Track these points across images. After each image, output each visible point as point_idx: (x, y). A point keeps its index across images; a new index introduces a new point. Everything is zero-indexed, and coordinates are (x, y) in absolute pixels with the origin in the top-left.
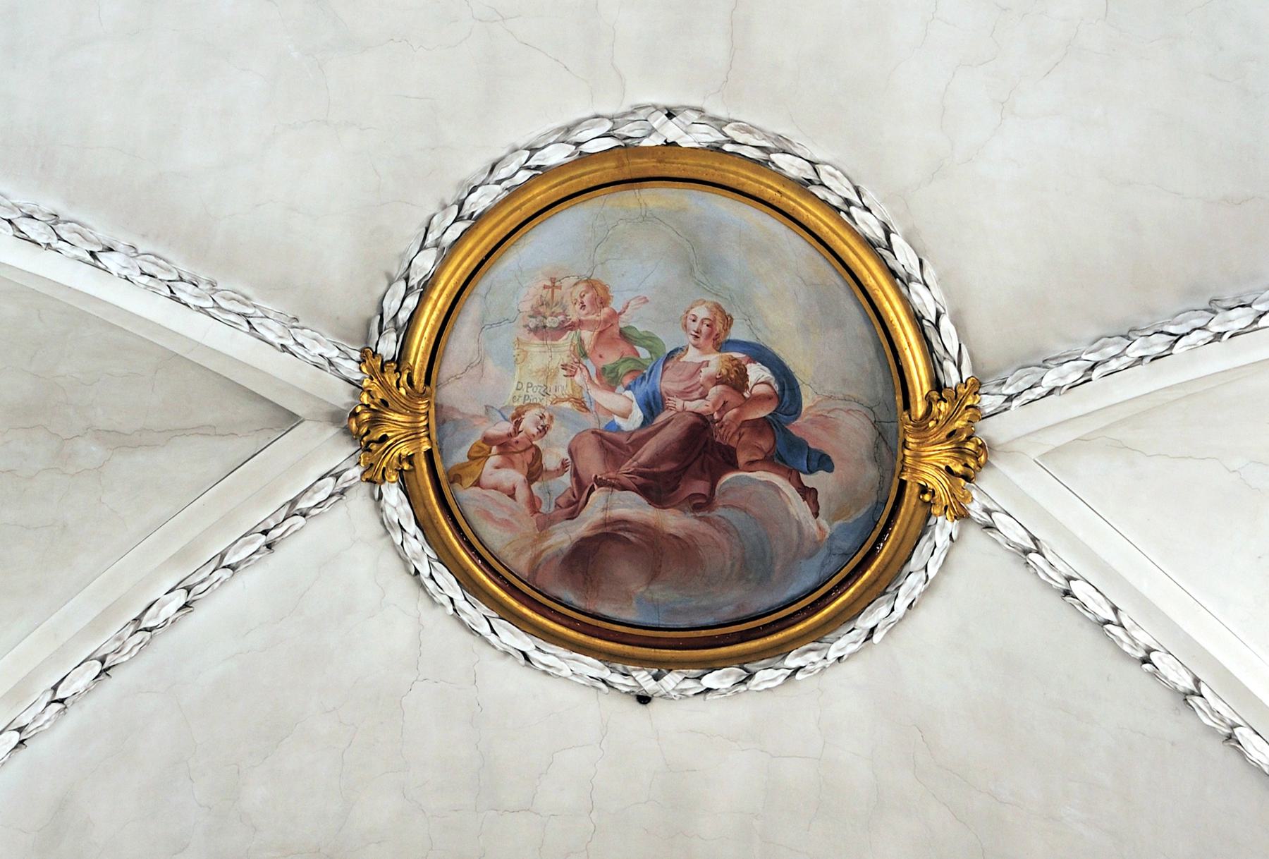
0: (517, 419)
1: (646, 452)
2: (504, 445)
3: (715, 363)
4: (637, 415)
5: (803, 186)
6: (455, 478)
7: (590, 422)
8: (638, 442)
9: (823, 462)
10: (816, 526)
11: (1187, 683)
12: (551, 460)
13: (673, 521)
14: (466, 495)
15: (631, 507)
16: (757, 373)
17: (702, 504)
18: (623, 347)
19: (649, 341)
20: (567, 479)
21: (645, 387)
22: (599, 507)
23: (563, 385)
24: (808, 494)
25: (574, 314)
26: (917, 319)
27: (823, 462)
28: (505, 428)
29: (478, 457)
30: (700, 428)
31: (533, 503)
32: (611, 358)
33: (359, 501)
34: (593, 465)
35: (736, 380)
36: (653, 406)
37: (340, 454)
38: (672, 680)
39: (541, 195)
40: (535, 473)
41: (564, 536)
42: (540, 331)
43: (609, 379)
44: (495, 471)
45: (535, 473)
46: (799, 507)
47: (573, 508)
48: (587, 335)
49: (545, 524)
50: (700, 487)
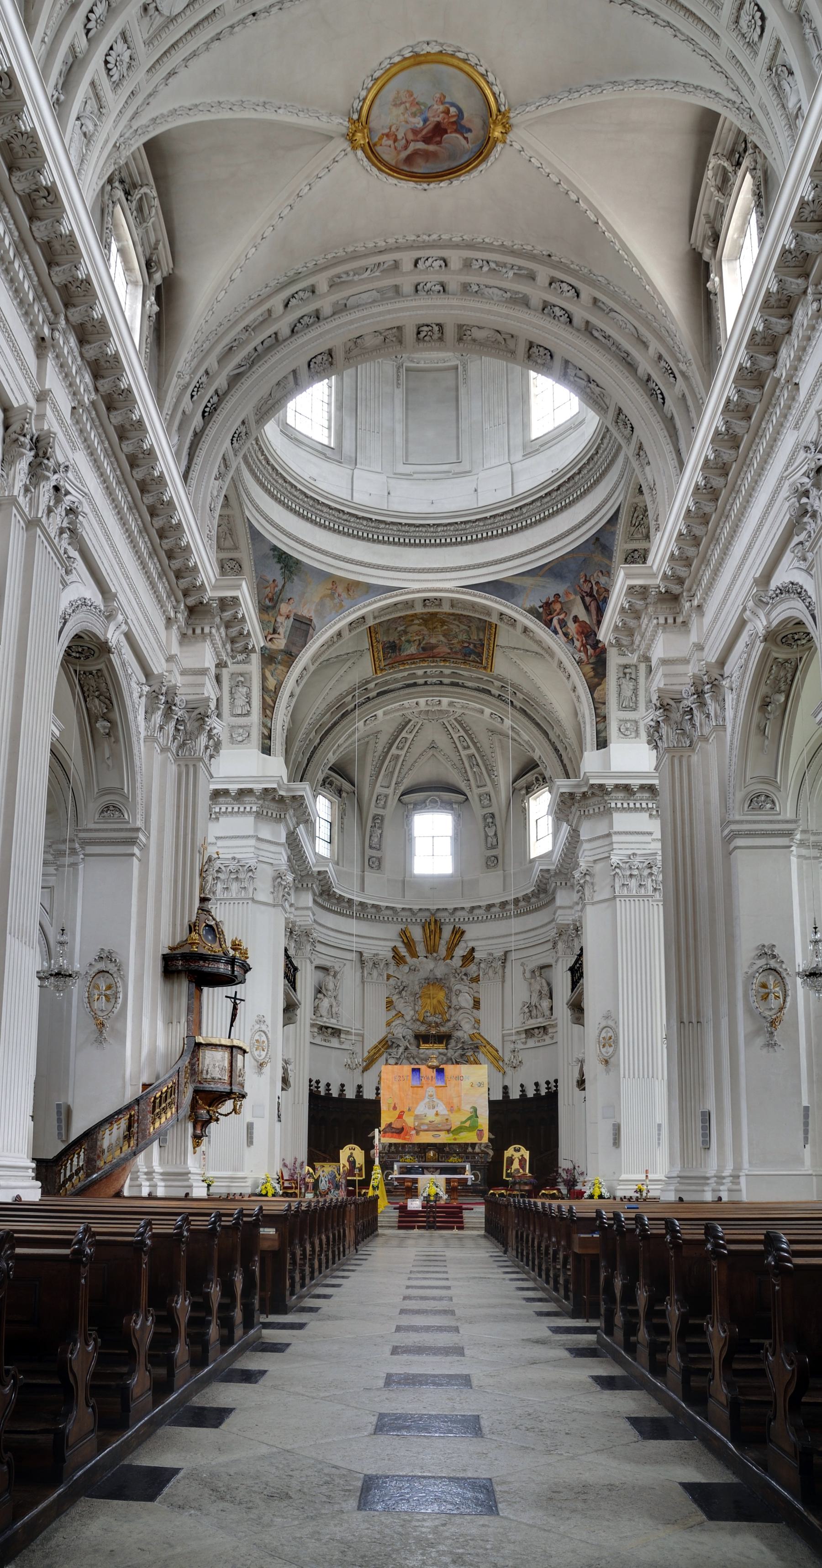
0: (390, 129)
1: (424, 132)
2: (387, 135)
3: (441, 108)
4: (422, 123)
5: (464, 61)
6: (375, 145)
7: (409, 126)
8: (422, 130)
9: (470, 130)
10: (467, 146)
11: (558, 181)
12: (399, 137)
13: (431, 148)
14: (378, 149)
15: (421, 145)
16: (453, 110)
17: (439, 143)
18: (418, 107)
19: (424, 104)
20: (404, 141)
21: (423, 116)
22: (412, 147)
23: (402, 118)
24: (466, 139)
25: (404, 100)
26: (494, 94)
27: (470, 130)
28: (386, 131)
29: (381, 139)
30: (438, 125)
31: (395, 148)
32: (414, 109)
33: (351, 155)
34: (410, 136)
35: (447, 112)
36: (425, 120)
37: (346, 145)
38: (432, 185)
39: (394, 70)
40: (395, 140)
41: (404, 154)
42: (395, 105)
43: (414, 115)
44: (385, 141)
45: (395, 140)
46: (463, 142)
47: (406, 148)
48: (408, 105)
49: (399, 152)
50: (438, 139)
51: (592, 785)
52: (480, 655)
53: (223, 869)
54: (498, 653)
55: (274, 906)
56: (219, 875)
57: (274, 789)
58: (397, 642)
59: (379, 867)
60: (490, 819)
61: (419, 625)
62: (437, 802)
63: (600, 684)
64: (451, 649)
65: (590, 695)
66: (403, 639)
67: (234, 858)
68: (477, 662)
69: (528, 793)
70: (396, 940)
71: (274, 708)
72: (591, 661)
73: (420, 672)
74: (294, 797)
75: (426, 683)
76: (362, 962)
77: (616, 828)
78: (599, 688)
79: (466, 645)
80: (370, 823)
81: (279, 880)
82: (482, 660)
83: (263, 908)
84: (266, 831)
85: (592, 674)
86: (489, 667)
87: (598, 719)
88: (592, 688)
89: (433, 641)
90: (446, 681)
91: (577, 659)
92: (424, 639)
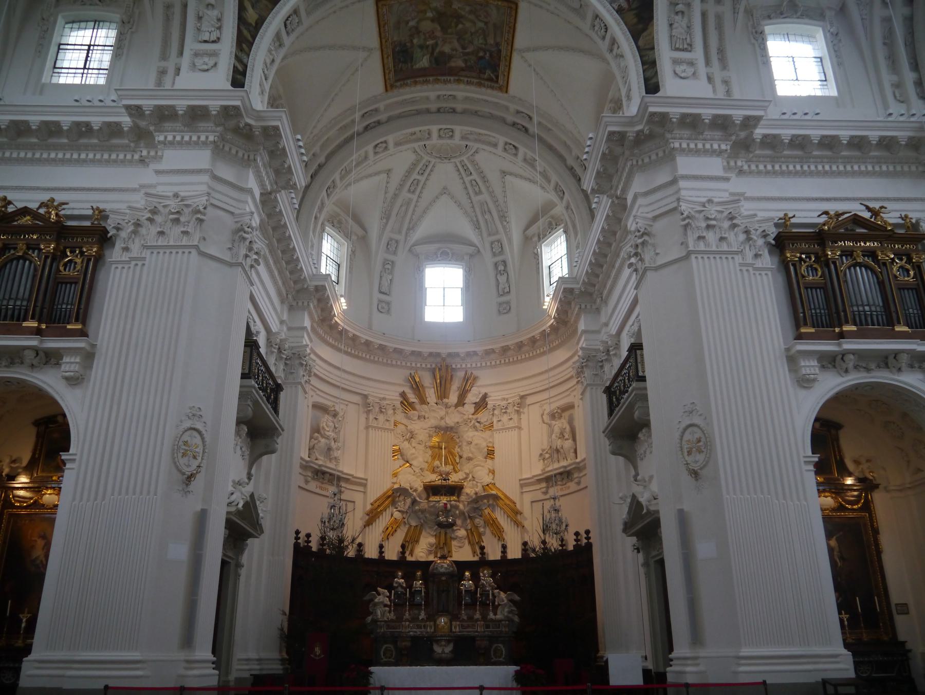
51: (653, 114)
52: (495, 68)
53: (161, 209)
54: (516, 60)
55: (231, 265)
56: (156, 217)
57: (236, 108)
58: (408, 44)
59: (388, 312)
60: (501, 268)
61: (433, 20)
62: (448, 254)
63: (644, 30)
64: (466, 61)
65: (633, 43)
66: (415, 41)
67: (176, 195)
68: (490, 80)
69: (539, 239)
70: (403, 385)
71: (252, 44)
72: (634, 6)
73: (432, 95)
74: (265, 129)
75: (438, 111)
76: (367, 405)
77: (681, 171)
78: (645, 34)
79: (481, 54)
80: (378, 267)
81: (242, 233)
82: (497, 77)
83: (214, 265)
84: (227, 172)
85: (635, 20)
86: (505, 89)
87: (646, 67)
88: (636, 35)
89: (447, 49)
90: (459, 107)
91: (616, 8)
92: (436, 44)
